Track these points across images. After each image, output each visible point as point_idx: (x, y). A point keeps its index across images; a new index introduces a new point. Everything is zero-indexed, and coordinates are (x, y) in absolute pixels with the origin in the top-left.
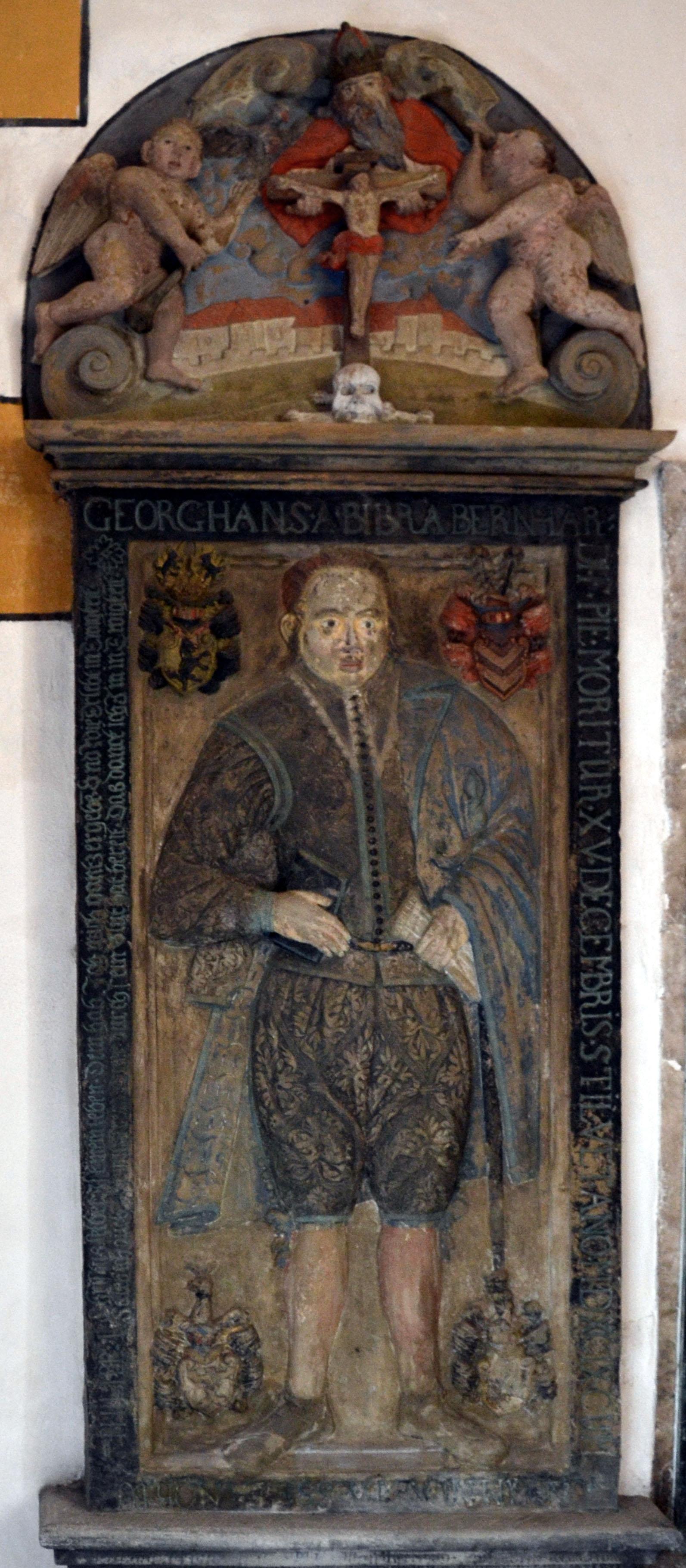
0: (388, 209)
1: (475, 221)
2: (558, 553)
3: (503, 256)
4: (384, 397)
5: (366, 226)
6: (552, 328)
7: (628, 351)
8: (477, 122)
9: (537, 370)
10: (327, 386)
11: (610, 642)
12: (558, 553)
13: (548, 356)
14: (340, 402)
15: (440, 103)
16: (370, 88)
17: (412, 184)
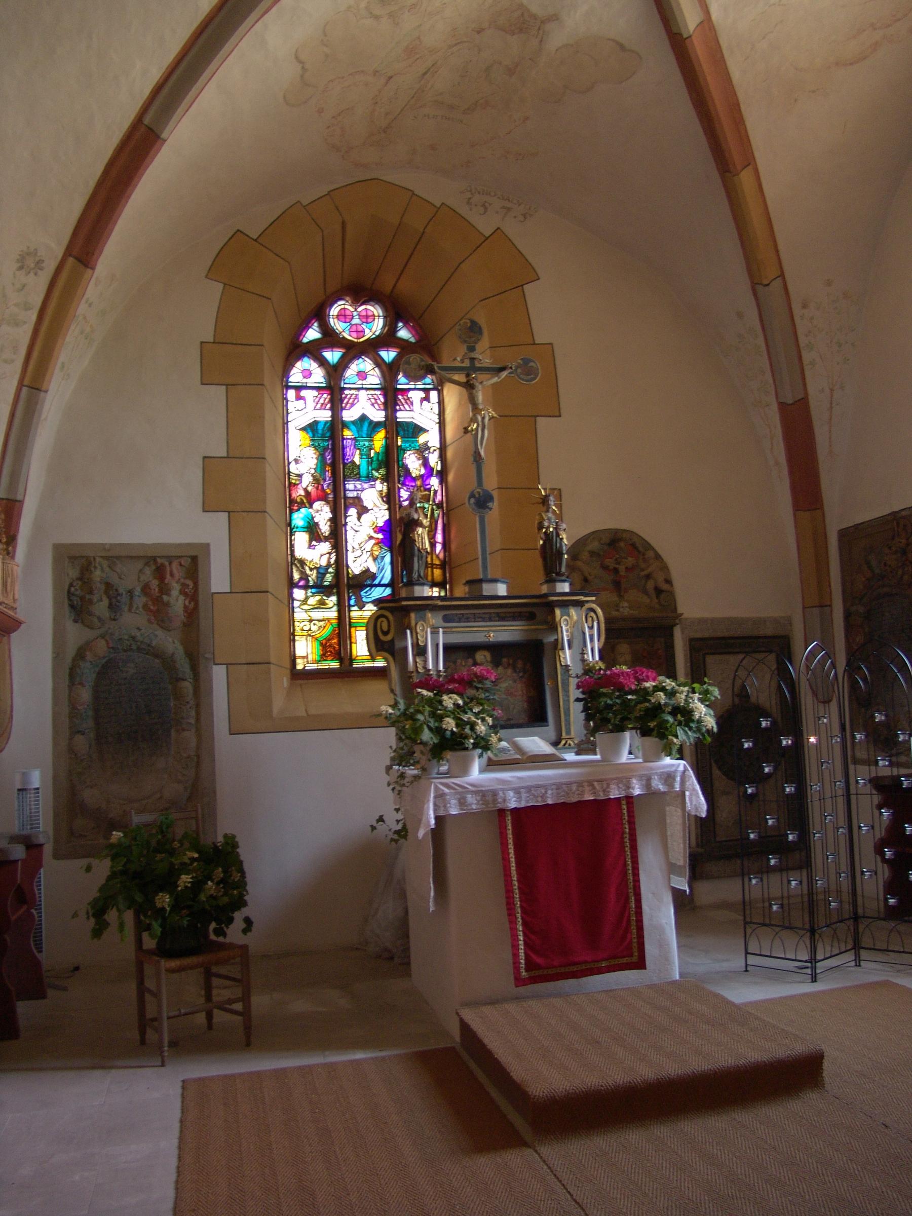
0: (627, 568)
1: (643, 570)
2: (662, 640)
3: (648, 577)
4: (629, 608)
5: (623, 573)
6: (658, 591)
7: (672, 594)
8: (641, 549)
9: (656, 601)
10: (617, 606)
11: (673, 657)
12: (662, 640)
13: (658, 597)
14: (621, 610)
15: (634, 546)
16: (622, 544)
17: (630, 561)
